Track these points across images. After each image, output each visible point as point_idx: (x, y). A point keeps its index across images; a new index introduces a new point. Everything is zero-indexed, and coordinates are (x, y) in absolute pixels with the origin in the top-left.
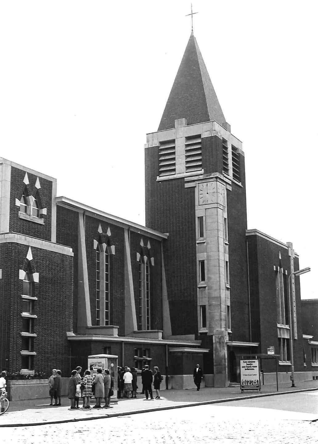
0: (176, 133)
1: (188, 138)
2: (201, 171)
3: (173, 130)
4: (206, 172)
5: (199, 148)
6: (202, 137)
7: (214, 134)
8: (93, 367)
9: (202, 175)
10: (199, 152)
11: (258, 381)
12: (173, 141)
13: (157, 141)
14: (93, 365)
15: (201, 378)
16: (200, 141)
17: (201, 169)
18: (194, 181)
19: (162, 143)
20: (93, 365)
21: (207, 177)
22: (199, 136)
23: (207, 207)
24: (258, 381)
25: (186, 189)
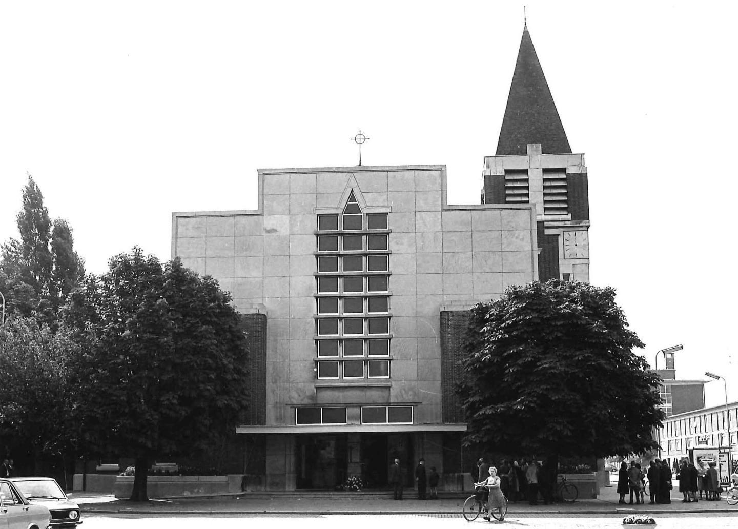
0: (529, 162)
1: (546, 171)
2: (567, 216)
3: (527, 158)
4: (573, 218)
5: (526, 186)
6: (567, 172)
7: (494, 173)
8: (702, 460)
9: (569, 221)
10: (564, 191)
11: (727, 478)
12: (525, 172)
13: (501, 169)
14: (701, 457)
15: (397, 458)
16: (564, 176)
17: (566, 213)
18: (557, 227)
19: (507, 172)
20: (701, 457)
21: (576, 224)
22: (563, 170)
23: (577, 262)
24: (727, 478)
25: (546, 237)
